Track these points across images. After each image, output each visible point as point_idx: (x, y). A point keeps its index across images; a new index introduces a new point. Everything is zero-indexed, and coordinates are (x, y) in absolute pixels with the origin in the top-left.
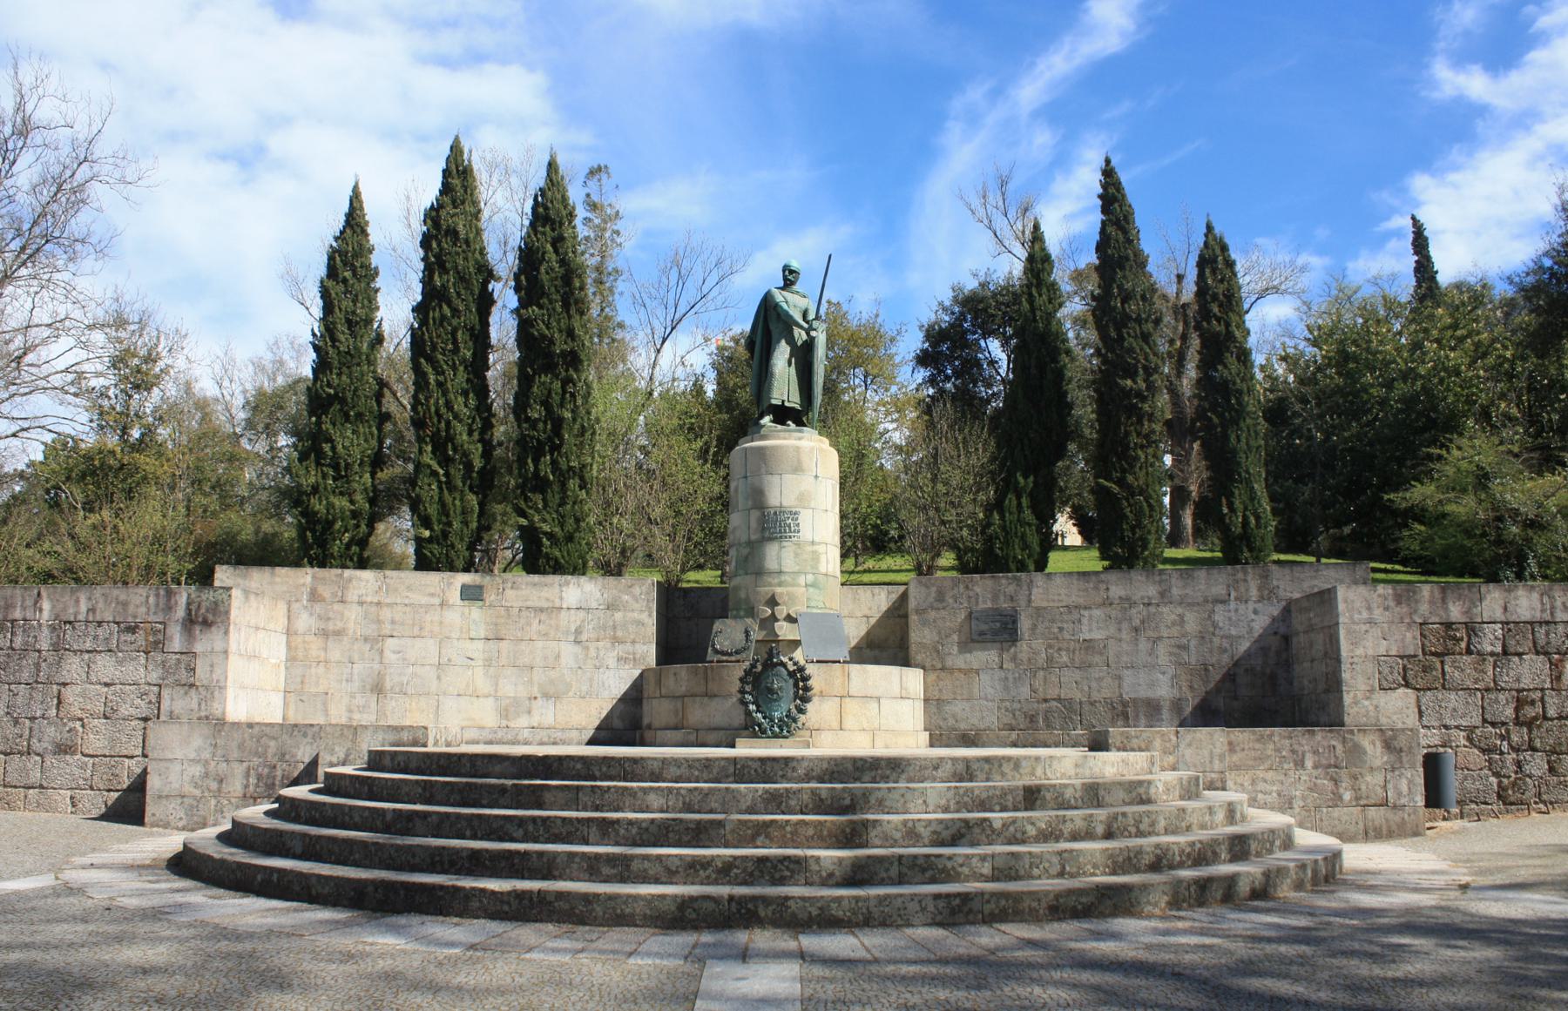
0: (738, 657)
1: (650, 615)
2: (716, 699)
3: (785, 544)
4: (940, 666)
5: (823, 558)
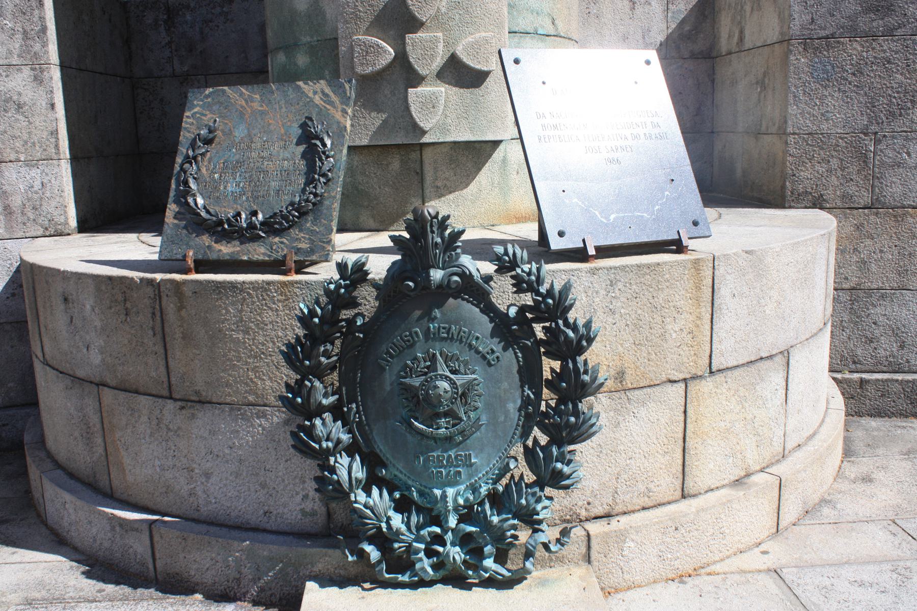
0: (279, 246)
1: (38, 79)
2: (204, 418)
4: (865, 198)
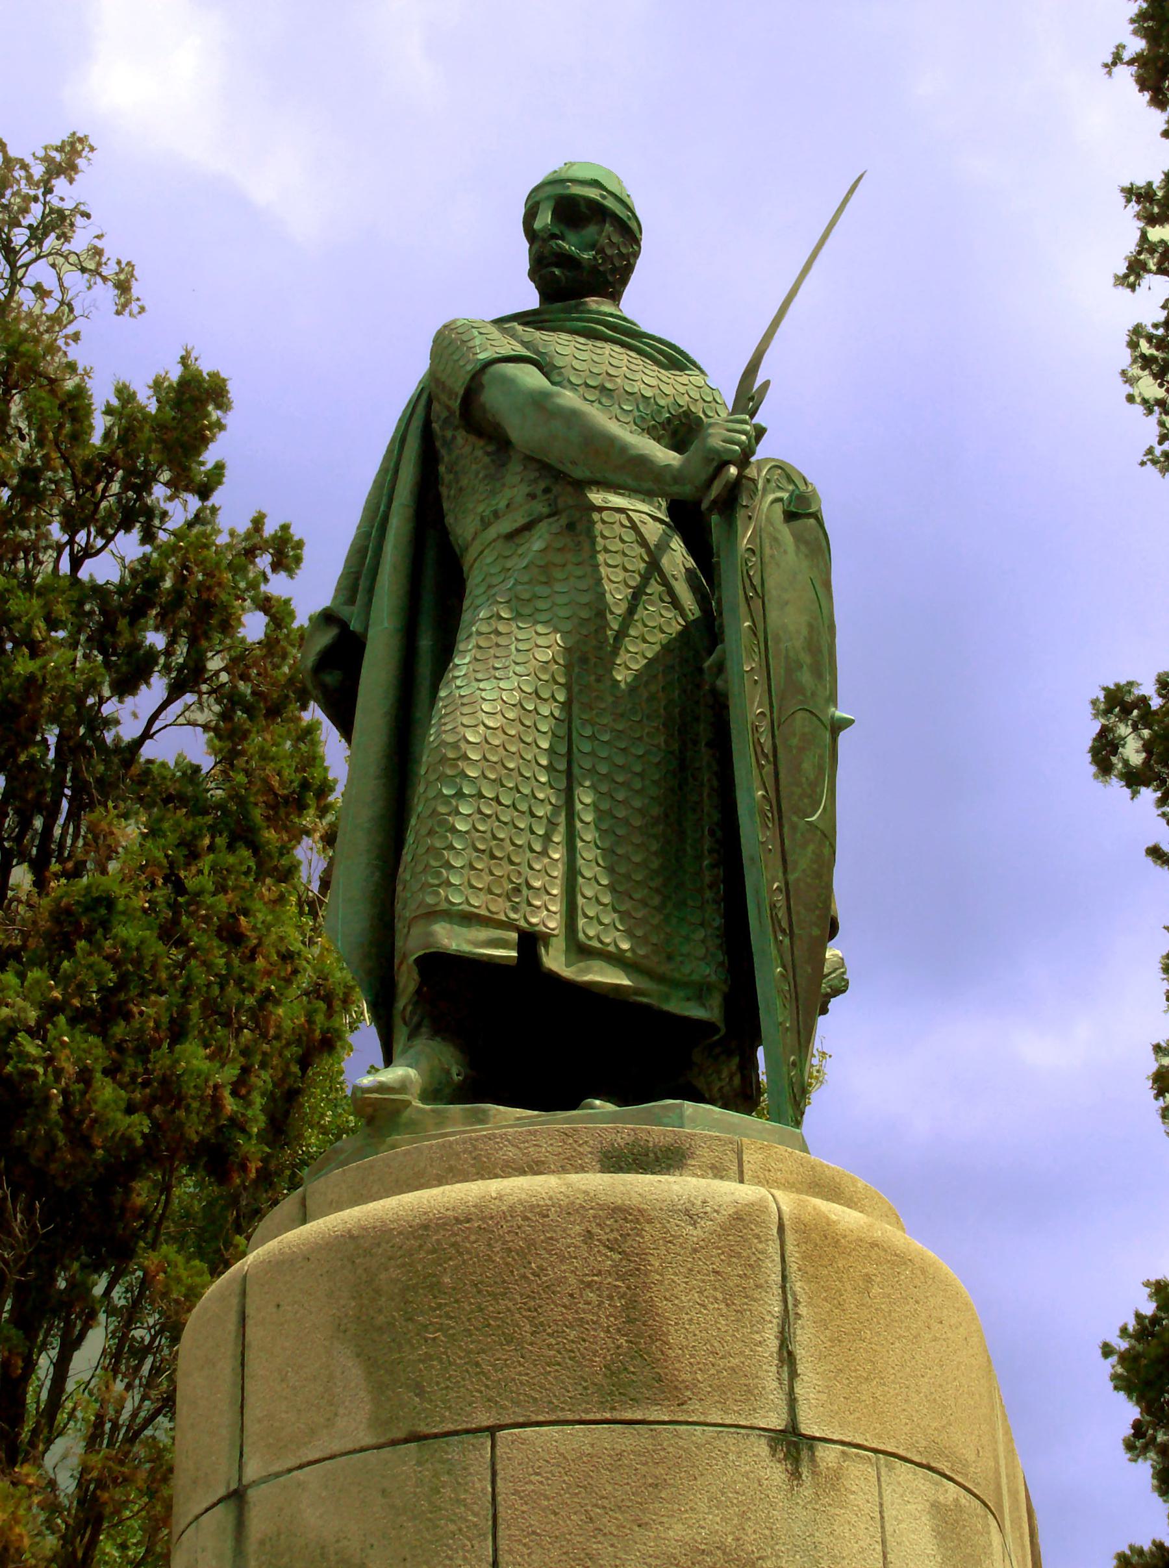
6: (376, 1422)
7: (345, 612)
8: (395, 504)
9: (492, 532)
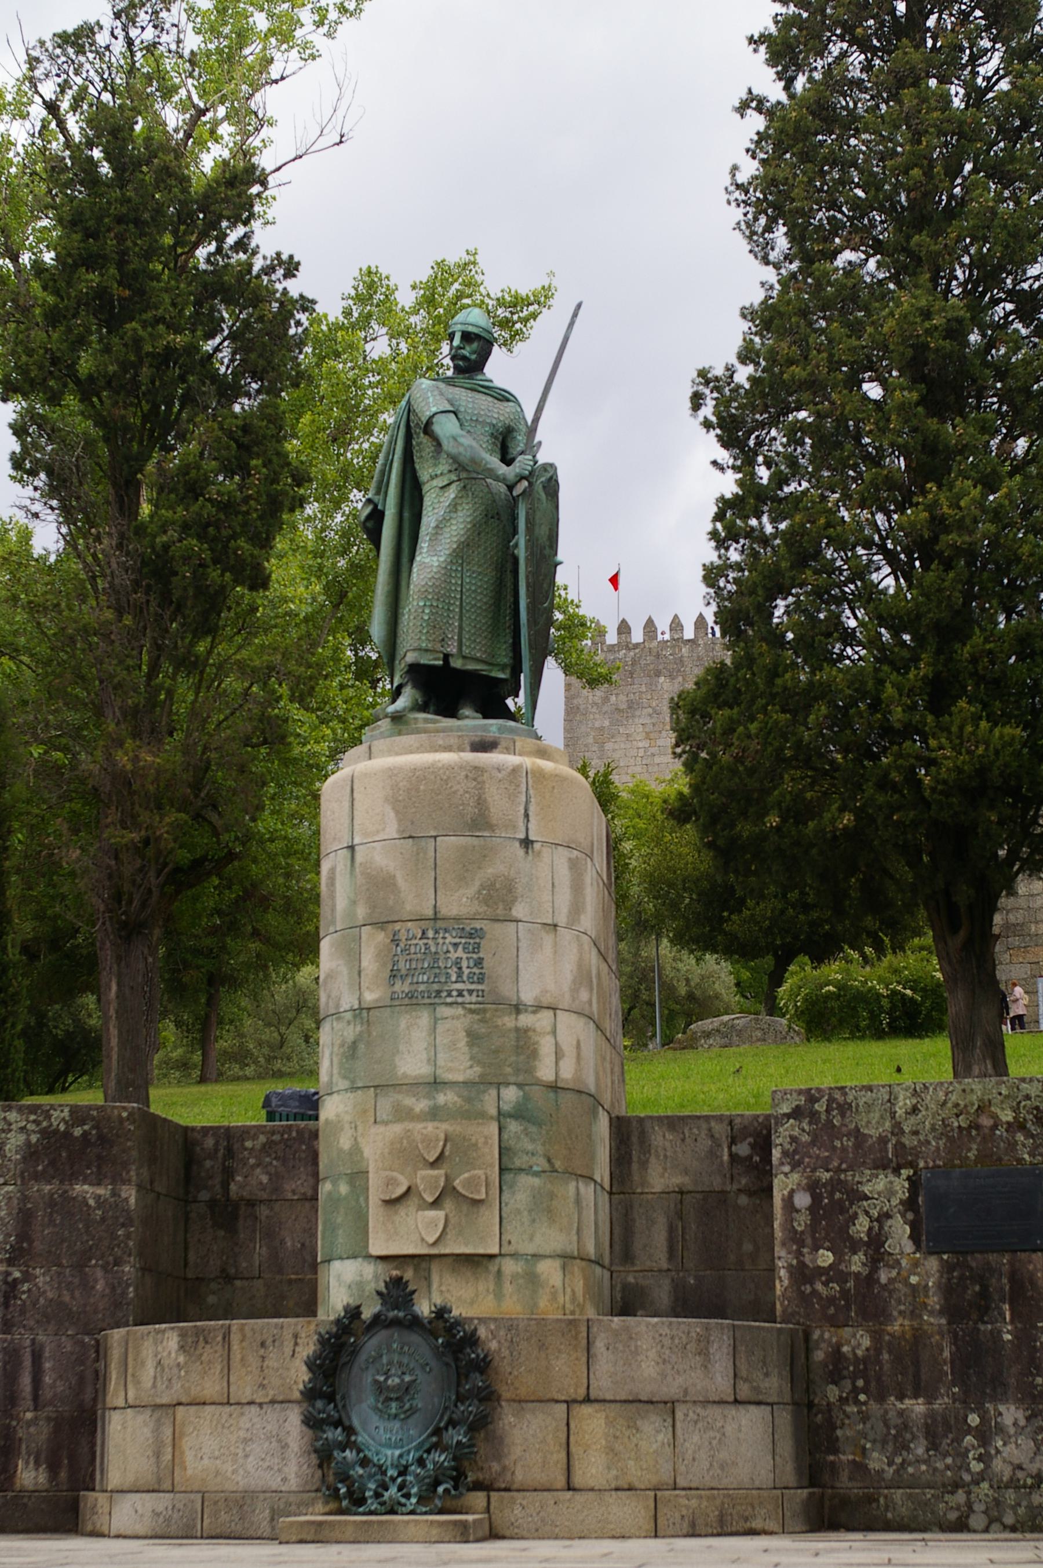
3: (444, 1011)
5: (546, 1047)
6: (398, 831)
7: (376, 499)
8: (396, 457)
9: (435, 483)
